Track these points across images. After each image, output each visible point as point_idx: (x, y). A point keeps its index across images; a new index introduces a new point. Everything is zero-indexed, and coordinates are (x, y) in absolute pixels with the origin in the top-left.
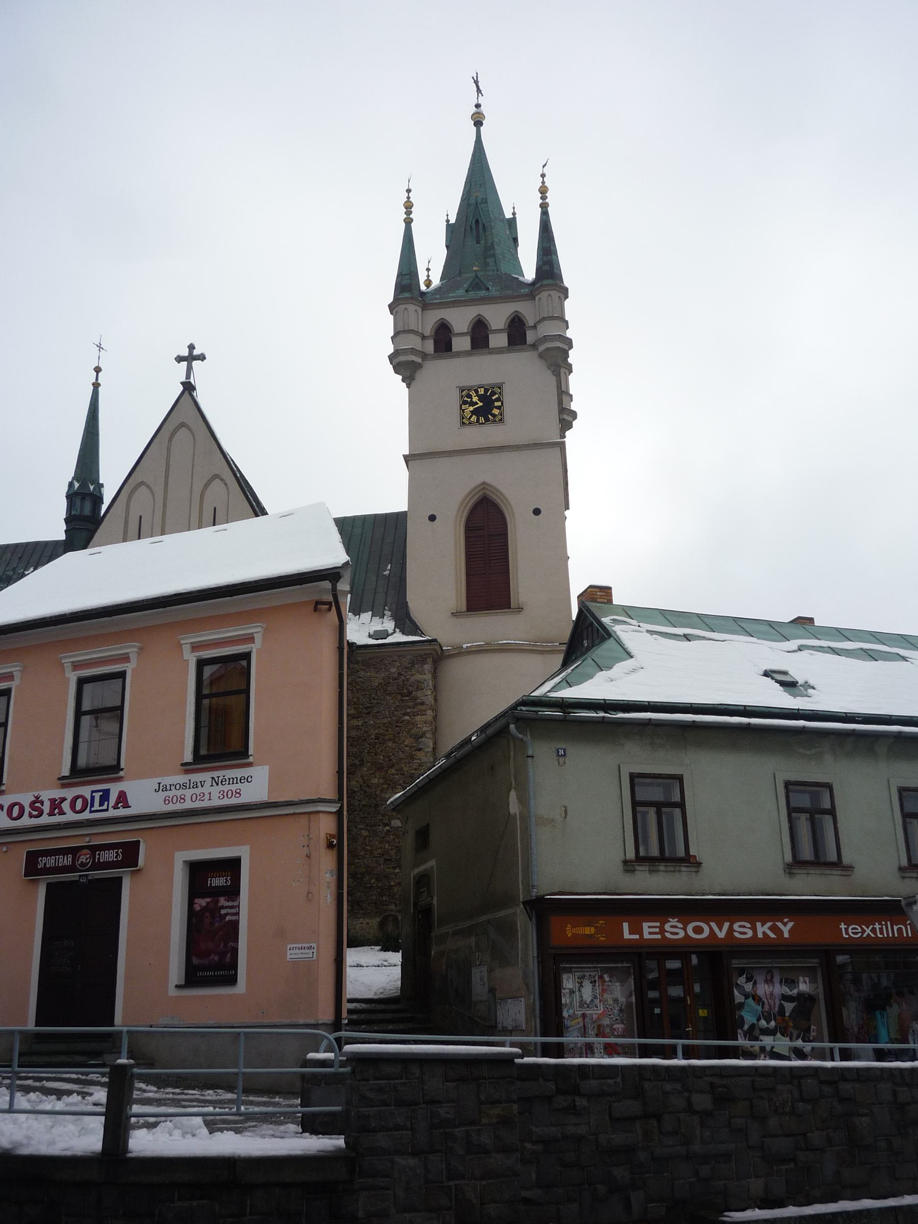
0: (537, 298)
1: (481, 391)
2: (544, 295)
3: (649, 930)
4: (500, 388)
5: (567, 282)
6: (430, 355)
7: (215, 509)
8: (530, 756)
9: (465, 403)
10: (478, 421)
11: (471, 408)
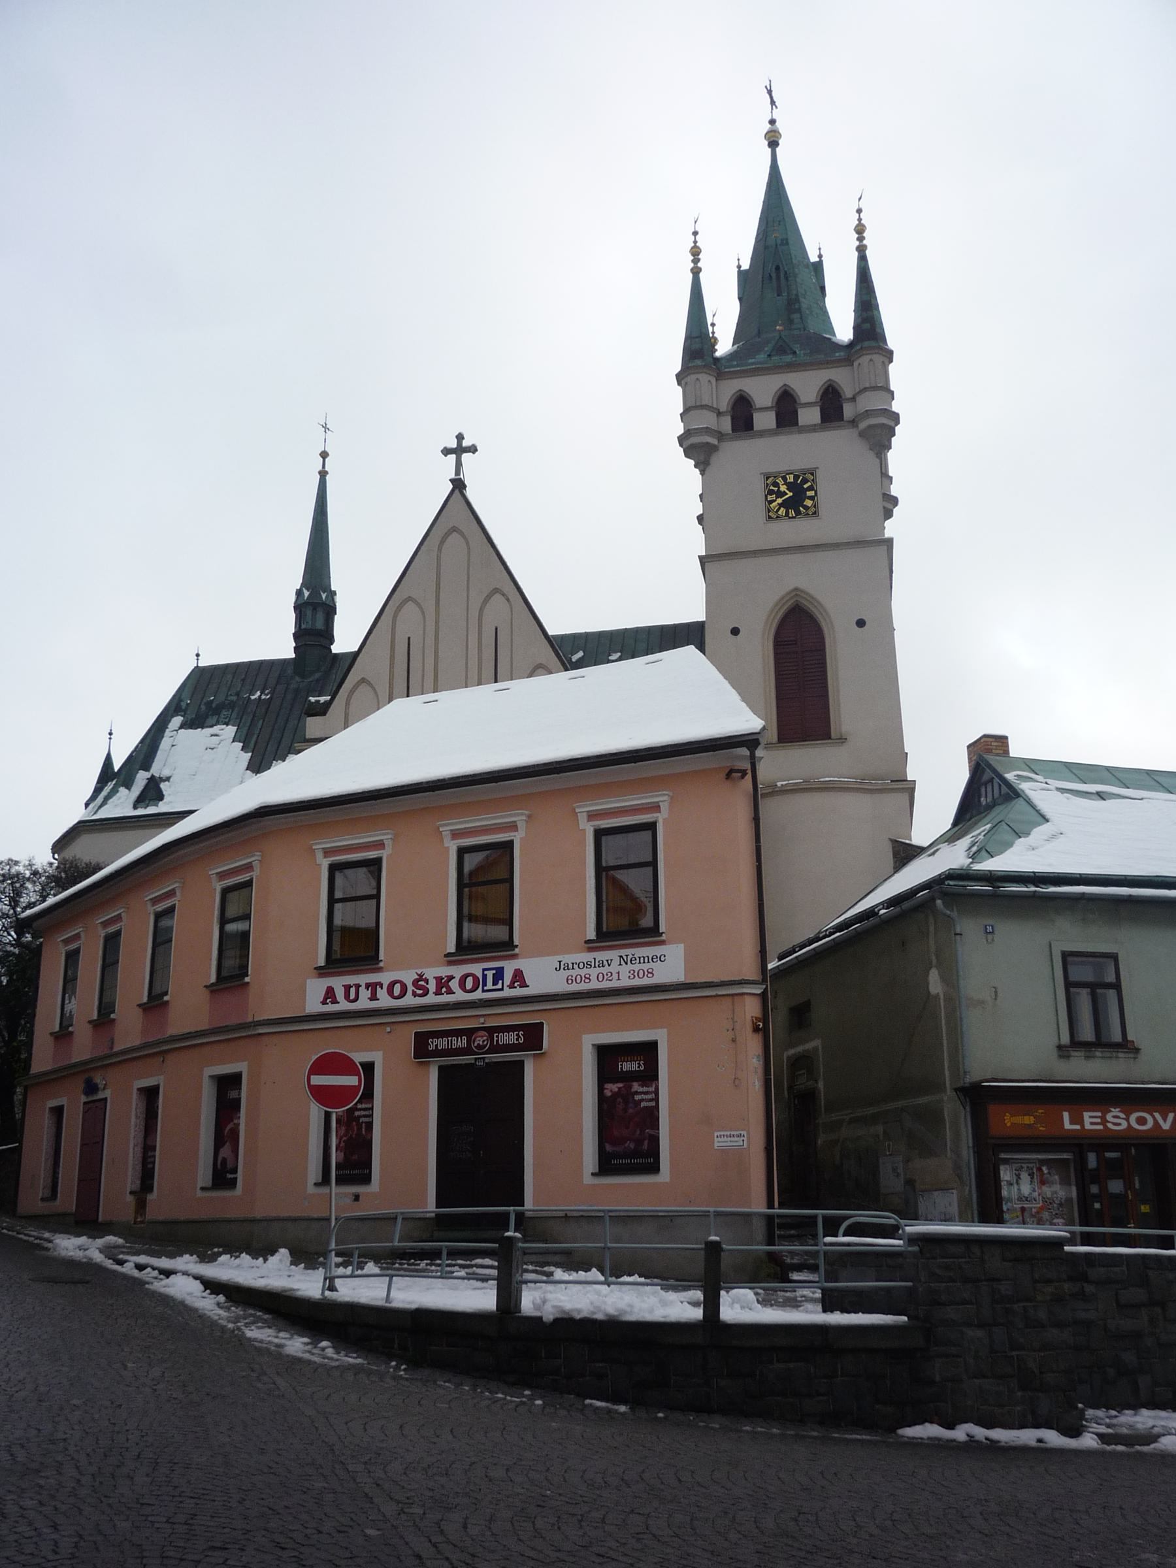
0: (856, 364)
1: (791, 479)
2: (865, 360)
3: (1090, 1120)
4: (812, 474)
5: (891, 343)
6: (727, 434)
7: (496, 629)
8: (958, 934)
9: (771, 492)
10: (787, 514)
11: (780, 501)
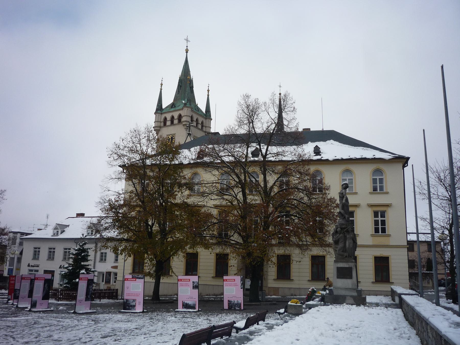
1: (171, 136)
2: (184, 109)
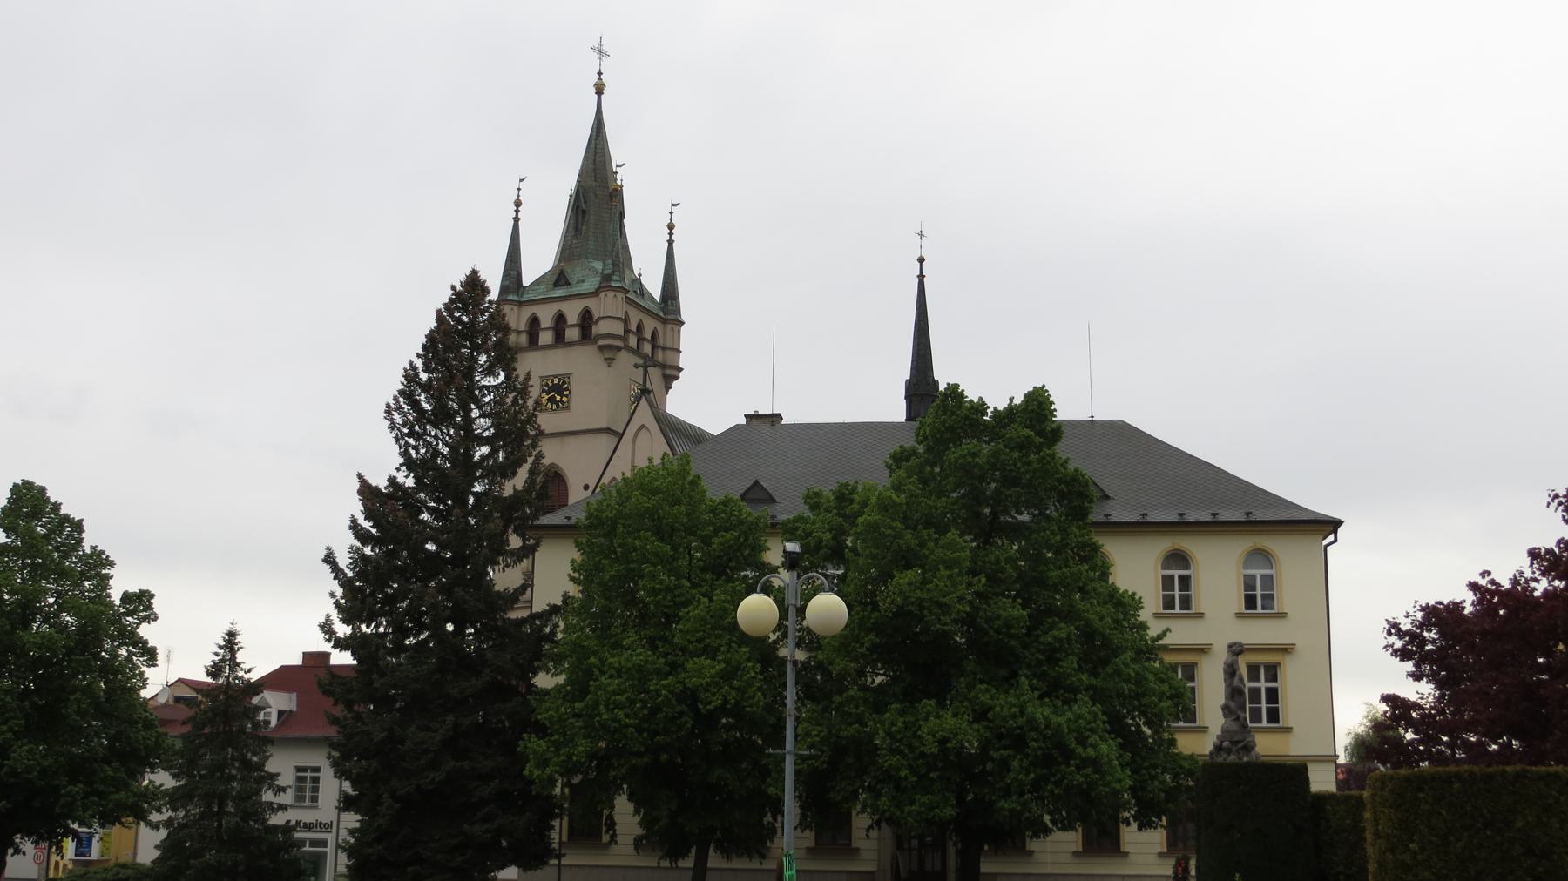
2: (602, 295)
10: (552, 406)
